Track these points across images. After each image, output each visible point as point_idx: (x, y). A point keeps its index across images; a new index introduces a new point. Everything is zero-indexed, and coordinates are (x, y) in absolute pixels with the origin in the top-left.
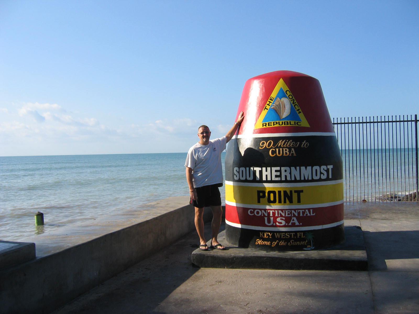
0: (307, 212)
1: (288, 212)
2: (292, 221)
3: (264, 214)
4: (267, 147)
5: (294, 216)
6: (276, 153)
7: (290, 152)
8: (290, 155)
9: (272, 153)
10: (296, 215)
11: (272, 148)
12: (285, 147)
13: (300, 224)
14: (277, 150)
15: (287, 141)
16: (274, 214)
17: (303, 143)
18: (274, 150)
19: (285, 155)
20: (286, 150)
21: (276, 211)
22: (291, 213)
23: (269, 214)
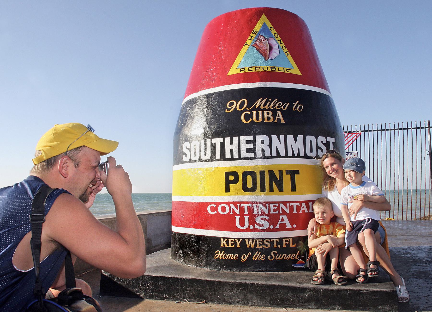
0: (303, 208)
1: (274, 206)
2: (280, 222)
3: (233, 211)
4: (238, 109)
5: (284, 213)
6: (252, 119)
7: (274, 115)
8: (276, 121)
9: (246, 119)
10: (287, 211)
11: (245, 110)
12: (267, 108)
13: (292, 226)
14: (254, 113)
15: (270, 100)
16: (250, 210)
17: (296, 104)
18: (249, 113)
19: (266, 121)
20: (268, 114)
21: (255, 206)
22: (278, 208)
23: (242, 209)
